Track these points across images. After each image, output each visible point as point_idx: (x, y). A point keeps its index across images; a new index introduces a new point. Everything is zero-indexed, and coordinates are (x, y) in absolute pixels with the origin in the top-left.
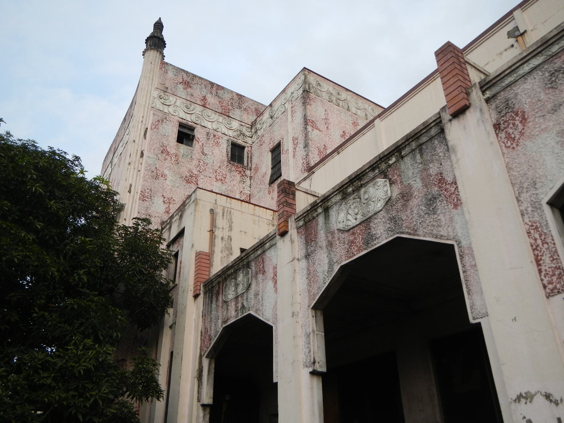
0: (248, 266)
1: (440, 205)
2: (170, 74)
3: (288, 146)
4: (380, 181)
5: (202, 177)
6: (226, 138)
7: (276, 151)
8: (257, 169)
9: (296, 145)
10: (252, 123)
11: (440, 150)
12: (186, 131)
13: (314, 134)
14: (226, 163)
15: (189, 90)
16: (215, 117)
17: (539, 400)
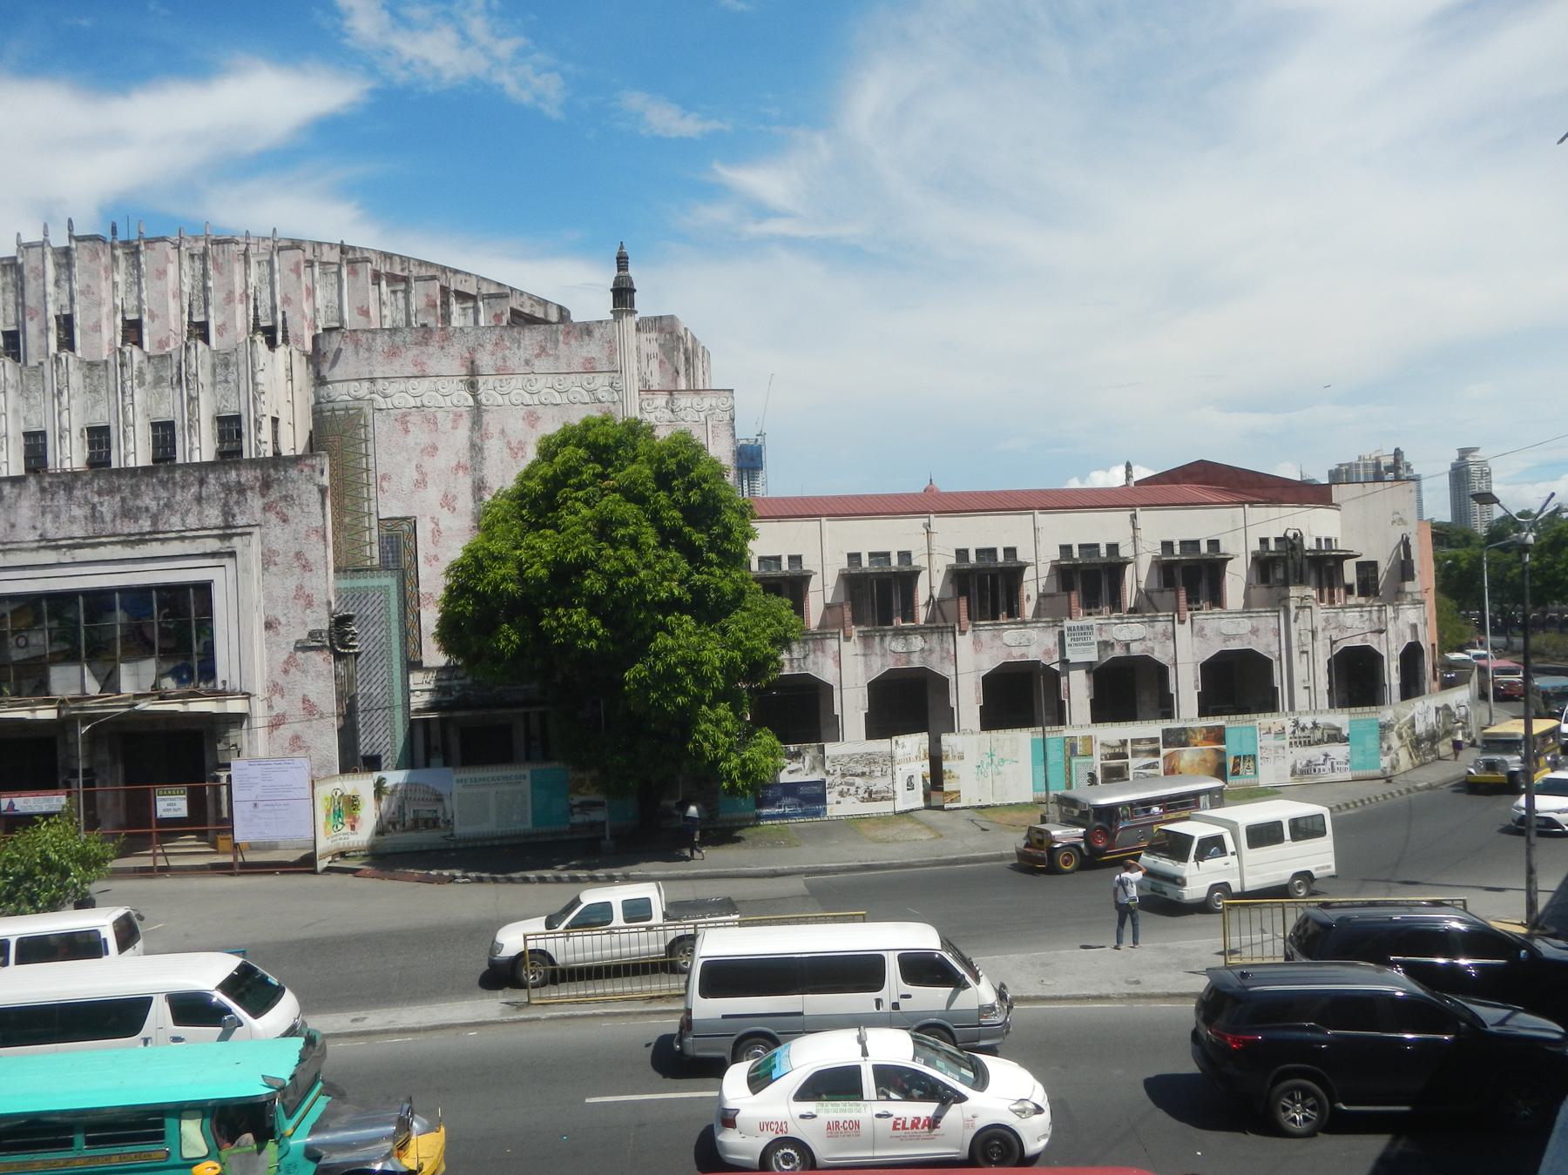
0: (805, 642)
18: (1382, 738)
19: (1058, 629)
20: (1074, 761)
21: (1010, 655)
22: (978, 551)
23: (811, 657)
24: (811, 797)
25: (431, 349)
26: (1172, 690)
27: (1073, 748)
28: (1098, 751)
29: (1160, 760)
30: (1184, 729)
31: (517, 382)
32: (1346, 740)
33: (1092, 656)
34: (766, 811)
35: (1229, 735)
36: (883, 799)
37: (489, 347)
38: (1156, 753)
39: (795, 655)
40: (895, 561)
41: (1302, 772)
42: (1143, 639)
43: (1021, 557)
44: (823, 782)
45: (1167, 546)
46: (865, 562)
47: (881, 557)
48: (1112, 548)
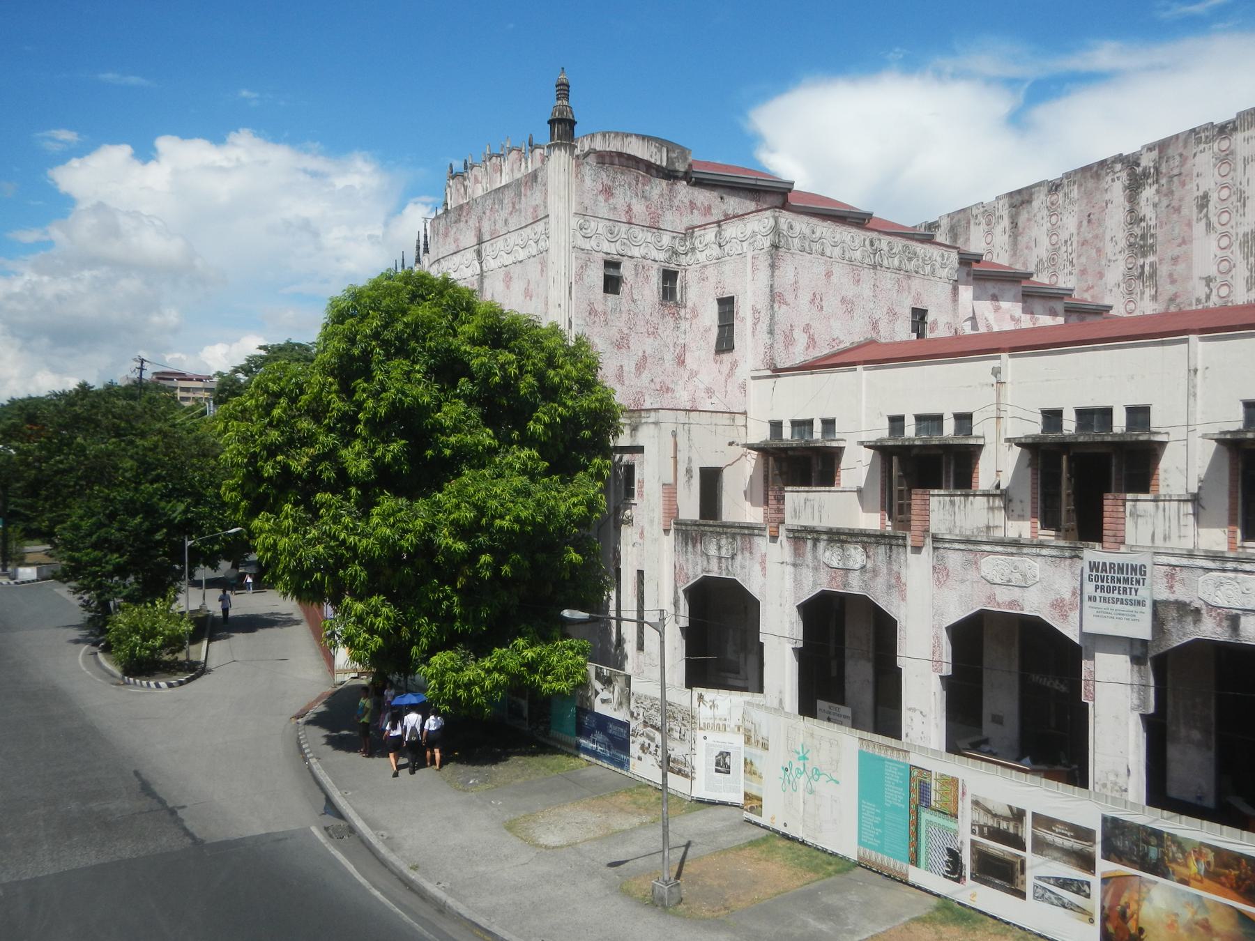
0: (734, 536)
1: (895, 593)
2: (588, 182)
3: (743, 310)
4: (861, 549)
6: (656, 266)
7: (727, 305)
9: (756, 321)
12: (612, 272)
13: (781, 311)
14: (657, 306)
16: (642, 235)
19: (1078, 564)
20: (925, 816)
21: (991, 598)
22: (1082, 414)
24: (617, 740)
25: (462, 224)
27: (924, 790)
28: (967, 815)
29: (1095, 881)
30: (1158, 834)
31: (500, 243)
33: (1141, 628)
34: (584, 742)
36: (679, 772)
37: (488, 212)
38: (1087, 863)
39: (724, 552)
40: (949, 428)
43: (1156, 421)
44: (626, 725)
46: (910, 430)
47: (931, 421)
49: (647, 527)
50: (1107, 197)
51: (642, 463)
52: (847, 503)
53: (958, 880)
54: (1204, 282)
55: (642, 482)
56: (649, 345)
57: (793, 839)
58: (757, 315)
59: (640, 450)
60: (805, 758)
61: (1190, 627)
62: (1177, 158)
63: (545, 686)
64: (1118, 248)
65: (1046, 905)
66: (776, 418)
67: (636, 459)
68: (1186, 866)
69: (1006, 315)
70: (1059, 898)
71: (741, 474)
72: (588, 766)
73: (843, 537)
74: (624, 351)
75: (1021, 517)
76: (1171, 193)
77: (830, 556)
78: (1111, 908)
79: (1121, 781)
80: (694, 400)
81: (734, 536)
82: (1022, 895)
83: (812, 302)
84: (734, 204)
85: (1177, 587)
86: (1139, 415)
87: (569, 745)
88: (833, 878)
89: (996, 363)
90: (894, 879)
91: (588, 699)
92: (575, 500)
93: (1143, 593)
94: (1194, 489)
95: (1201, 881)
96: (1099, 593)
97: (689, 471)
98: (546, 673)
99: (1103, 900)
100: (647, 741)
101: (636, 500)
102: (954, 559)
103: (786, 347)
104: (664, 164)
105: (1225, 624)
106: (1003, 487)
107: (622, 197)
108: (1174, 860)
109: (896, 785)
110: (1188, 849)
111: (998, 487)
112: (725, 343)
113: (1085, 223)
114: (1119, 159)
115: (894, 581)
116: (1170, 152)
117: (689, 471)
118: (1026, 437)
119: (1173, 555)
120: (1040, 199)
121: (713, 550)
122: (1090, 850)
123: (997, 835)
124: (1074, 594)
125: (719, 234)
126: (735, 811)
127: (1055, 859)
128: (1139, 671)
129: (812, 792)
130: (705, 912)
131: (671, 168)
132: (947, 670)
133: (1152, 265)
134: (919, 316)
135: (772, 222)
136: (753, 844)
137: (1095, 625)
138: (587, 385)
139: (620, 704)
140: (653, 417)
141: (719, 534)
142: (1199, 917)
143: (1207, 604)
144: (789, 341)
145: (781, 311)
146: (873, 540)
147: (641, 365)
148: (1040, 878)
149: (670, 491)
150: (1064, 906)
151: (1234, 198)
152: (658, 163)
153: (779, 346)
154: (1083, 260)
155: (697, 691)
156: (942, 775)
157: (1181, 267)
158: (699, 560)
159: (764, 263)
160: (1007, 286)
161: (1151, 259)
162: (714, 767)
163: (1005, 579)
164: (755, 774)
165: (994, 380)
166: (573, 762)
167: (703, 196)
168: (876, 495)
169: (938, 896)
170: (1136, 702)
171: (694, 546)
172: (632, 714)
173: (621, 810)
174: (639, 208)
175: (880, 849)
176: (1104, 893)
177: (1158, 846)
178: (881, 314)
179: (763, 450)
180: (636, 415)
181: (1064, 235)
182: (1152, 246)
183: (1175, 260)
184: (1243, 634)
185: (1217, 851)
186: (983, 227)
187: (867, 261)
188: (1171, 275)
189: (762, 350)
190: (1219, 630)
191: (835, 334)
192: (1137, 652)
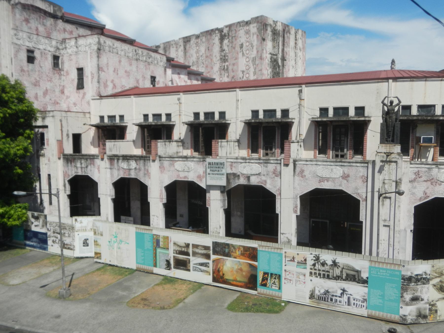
0: (87, 159)
4: (134, 162)
5: (41, 81)
6: (50, 53)
7: (80, 71)
8: (68, 73)
10: (63, 39)
11: (149, 164)
12: (31, 54)
13: (102, 74)
14: (51, 70)
15: (29, 25)
16: (43, 40)
17: (155, 217)
18: (404, 289)
19: (205, 163)
20: (159, 250)
21: (178, 176)
23: (89, 167)
24: (42, 240)
26: (278, 211)
27: (158, 242)
28: (172, 248)
29: (211, 262)
30: (228, 245)
32: (365, 282)
33: (223, 182)
34: (28, 242)
35: (260, 256)
36: (69, 248)
39: (83, 166)
40: (164, 119)
41: (320, 298)
42: (259, 174)
43: (227, 117)
44: (46, 234)
45: (324, 111)
46: (151, 119)
47: (157, 116)
48: (285, 113)
49: (51, 157)
50: (214, 42)
51: (47, 132)
52: (129, 145)
53: (169, 269)
54: (242, 72)
55: (48, 140)
56: (49, 85)
57: (113, 266)
58: (93, 75)
59: (46, 127)
60: (116, 237)
61: (237, 181)
62: (234, 32)
63: (9, 223)
64: (217, 59)
65: (196, 272)
66: (102, 115)
67: (44, 130)
68: (236, 253)
69: (182, 80)
70: (200, 269)
71: (89, 136)
72: (31, 251)
73: (128, 158)
74: (38, 87)
75: (188, 149)
76: (232, 42)
77: (124, 165)
78: (215, 269)
79: (218, 230)
80: (68, 107)
81: (87, 159)
82: (189, 270)
83: (114, 71)
84: (82, 31)
85: (233, 169)
86: (222, 114)
87: (22, 245)
88: (128, 276)
89: (179, 96)
90: (149, 273)
91: (29, 226)
92: (18, 148)
93: (224, 171)
94: (238, 138)
95: (240, 257)
96: (211, 172)
97: (68, 135)
98: (9, 218)
99: (213, 267)
100: (55, 239)
101: (46, 146)
102: (166, 163)
103: (105, 88)
104: (52, 12)
105: (246, 179)
106: (182, 138)
107: (34, 24)
108: (232, 252)
109: (149, 241)
110: (236, 248)
111: (180, 138)
112: (80, 86)
113: (207, 50)
114: (217, 29)
115: (146, 172)
116: (232, 28)
117: (68, 135)
118: (189, 122)
119: (232, 159)
120: (193, 41)
121: (79, 165)
122: (209, 253)
123: (181, 253)
124: (204, 173)
125: (76, 42)
126: (91, 259)
127: (199, 257)
128: (223, 196)
129: (119, 248)
130: (80, 297)
131: (55, 14)
132: (165, 201)
133: (227, 66)
134: (153, 79)
135: (97, 40)
136: (98, 270)
137: (210, 182)
138: (21, 100)
139: (43, 226)
140: (51, 114)
141: (81, 159)
142: (239, 267)
143: (241, 173)
144: (106, 86)
145: (102, 74)
146: (138, 158)
147: (46, 93)
148: (194, 264)
149: (60, 143)
150: (202, 271)
151: (250, 46)
152: (49, 11)
153: (102, 88)
154: (207, 62)
155: (74, 218)
156: (163, 236)
157: (235, 67)
158: (73, 168)
159: (95, 55)
160: (183, 70)
161: (227, 64)
162: (82, 245)
163: (183, 169)
164: (98, 245)
165: (178, 102)
166: (24, 251)
167: (69, 27)
168: (139, 143)
169: (163, 276)
170: (222, 205)
171: (71, 163)
172: (48, 229)
173: (45, 266)
174: (41, 29)
175: (144, 264)
176: (213, 265)
177: (228, 248)
178: (140, 77)
179: (97, 127)
180: (44, 113)
181: (201, 54)
182: (227, 60)
183: (234, 64)
184: (251, 181)
185: (244, 247)
186: (175, 49)
187: (134, 57)
188: (232, 69)
189: (95, 89)
190: (245, 181)
191: (124, 83)
192: (222, 190)
